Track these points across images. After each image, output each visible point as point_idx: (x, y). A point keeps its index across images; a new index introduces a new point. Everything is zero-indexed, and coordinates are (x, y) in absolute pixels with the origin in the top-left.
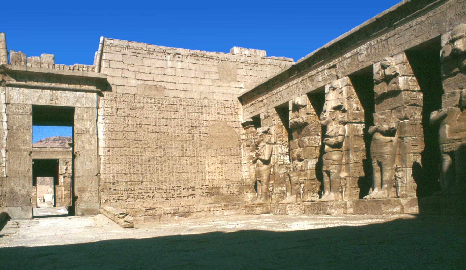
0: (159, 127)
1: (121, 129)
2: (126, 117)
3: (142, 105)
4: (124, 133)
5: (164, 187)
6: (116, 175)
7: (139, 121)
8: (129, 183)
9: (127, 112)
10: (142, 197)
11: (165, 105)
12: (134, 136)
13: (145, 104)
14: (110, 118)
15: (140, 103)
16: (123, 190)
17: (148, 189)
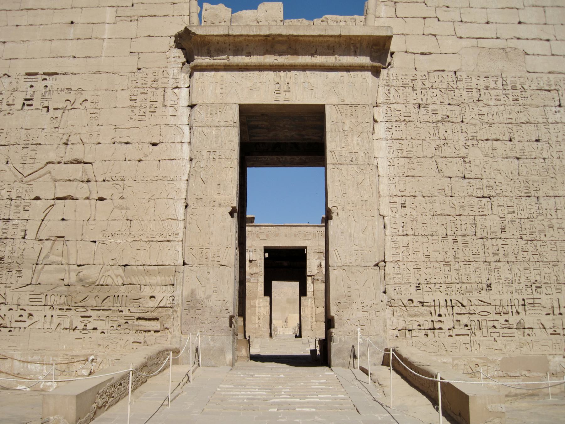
0: (519, 146)
1: (430, 151)
2: (440, 124)
3: (475, 94)
4: (439, 160)
5: (545, 300)
6: (422, 265)
7: (471, 131)
8: (455, 287)
9: (443, 112)
10: (491, 324)
11: (529, 93)
12: (462, 168)
13: (483, 91)
14: (404, 129)
15: (469, 89)
16: (443, 303)
17: (505, 303)
